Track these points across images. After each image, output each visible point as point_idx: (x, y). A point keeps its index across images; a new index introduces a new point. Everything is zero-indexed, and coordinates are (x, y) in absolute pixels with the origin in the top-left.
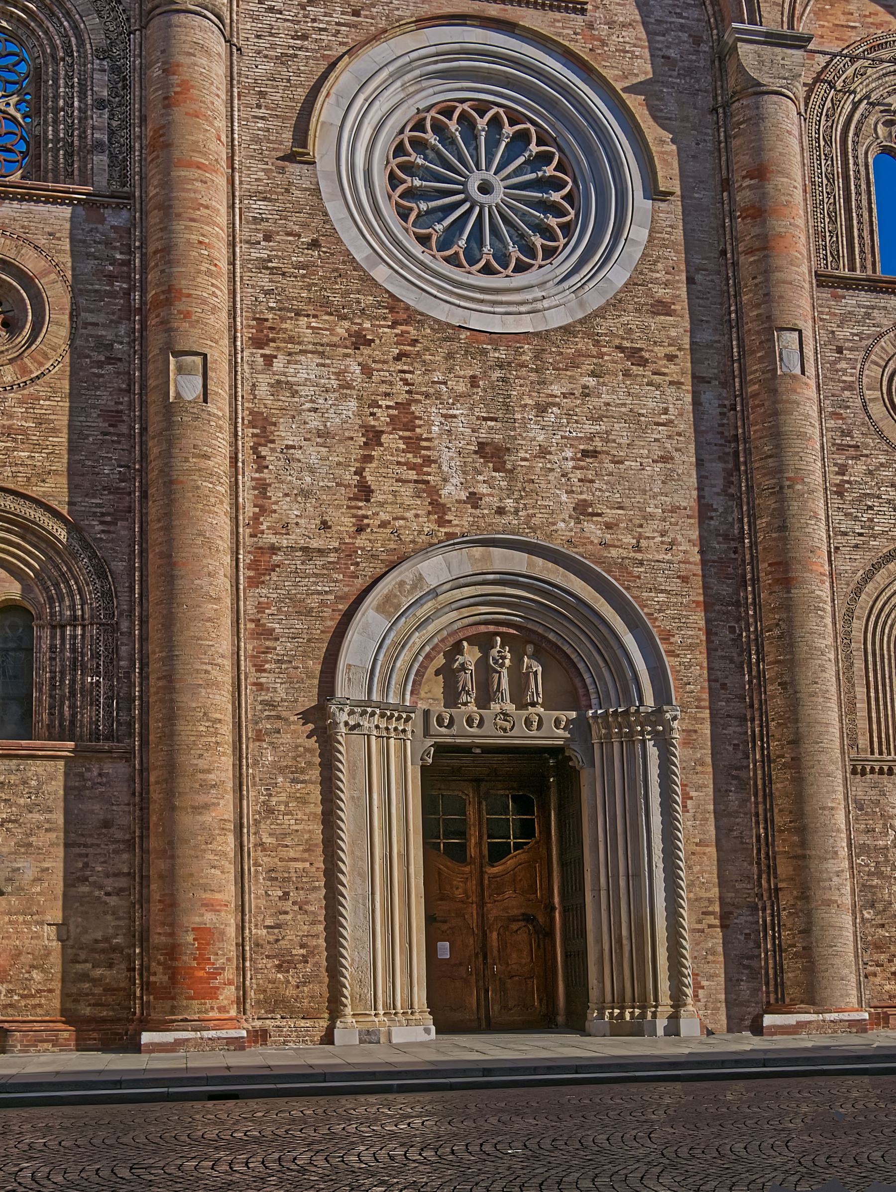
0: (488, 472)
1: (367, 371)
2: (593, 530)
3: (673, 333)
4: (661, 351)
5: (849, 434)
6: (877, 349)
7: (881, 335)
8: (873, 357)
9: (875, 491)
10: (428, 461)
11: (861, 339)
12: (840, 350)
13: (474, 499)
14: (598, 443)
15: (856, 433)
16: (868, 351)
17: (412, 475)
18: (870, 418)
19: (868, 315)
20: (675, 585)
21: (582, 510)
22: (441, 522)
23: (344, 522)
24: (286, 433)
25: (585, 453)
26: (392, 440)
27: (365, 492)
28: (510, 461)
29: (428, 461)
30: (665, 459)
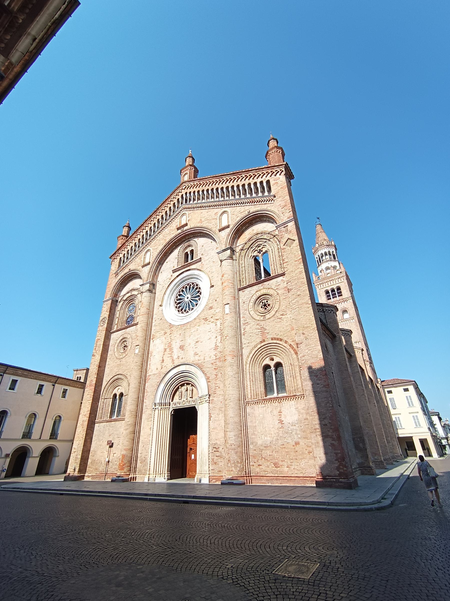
0: (181, 351)
1: (165, 338)
2: (197, 358)
3: (212, 312)
4: (210, 317)
5: (246, 320)
6: (252, 299)
9: (252, 332)
10: (173, 352)
12: (244, 303)
13: (178, 357)
14: (198, 340)
15: (247, 320)
17: (170, 355)
19: (250, 293)
20: (211, 366)
21: (196, 354)
22: (173, 363)
23: (159, 367)
24: (153, 354)
25: (196, 342)
26: (168, 350)
27: (163, 360)
28: (184, 347)
29: (173, 352)
30: (210, 339)
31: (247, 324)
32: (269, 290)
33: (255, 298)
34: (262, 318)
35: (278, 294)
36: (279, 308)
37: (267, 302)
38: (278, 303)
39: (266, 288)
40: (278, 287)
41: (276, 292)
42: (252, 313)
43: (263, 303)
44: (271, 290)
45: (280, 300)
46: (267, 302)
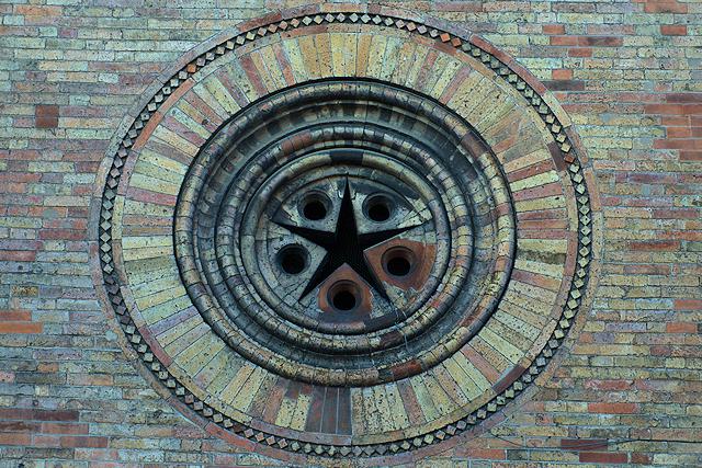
7: (195, 64)
8: (161, 133)
11: (127, 81)
12: (47, 118)
16: (144, 119)
18: (126, 319)
31: (49, 435)
32: (449, 65)
33: (219, 96)
34: (294, 414)
35: (564, 157)
36: (555, 347)
37: (378, 210)
38: (556, 272)
39: (414, 30)
40: (582, 68)
41: (546, 114)
42: (156, 295)
43: (315, 208)
44: (480, 78)
45: (582, 243)
46: (378, 210)
